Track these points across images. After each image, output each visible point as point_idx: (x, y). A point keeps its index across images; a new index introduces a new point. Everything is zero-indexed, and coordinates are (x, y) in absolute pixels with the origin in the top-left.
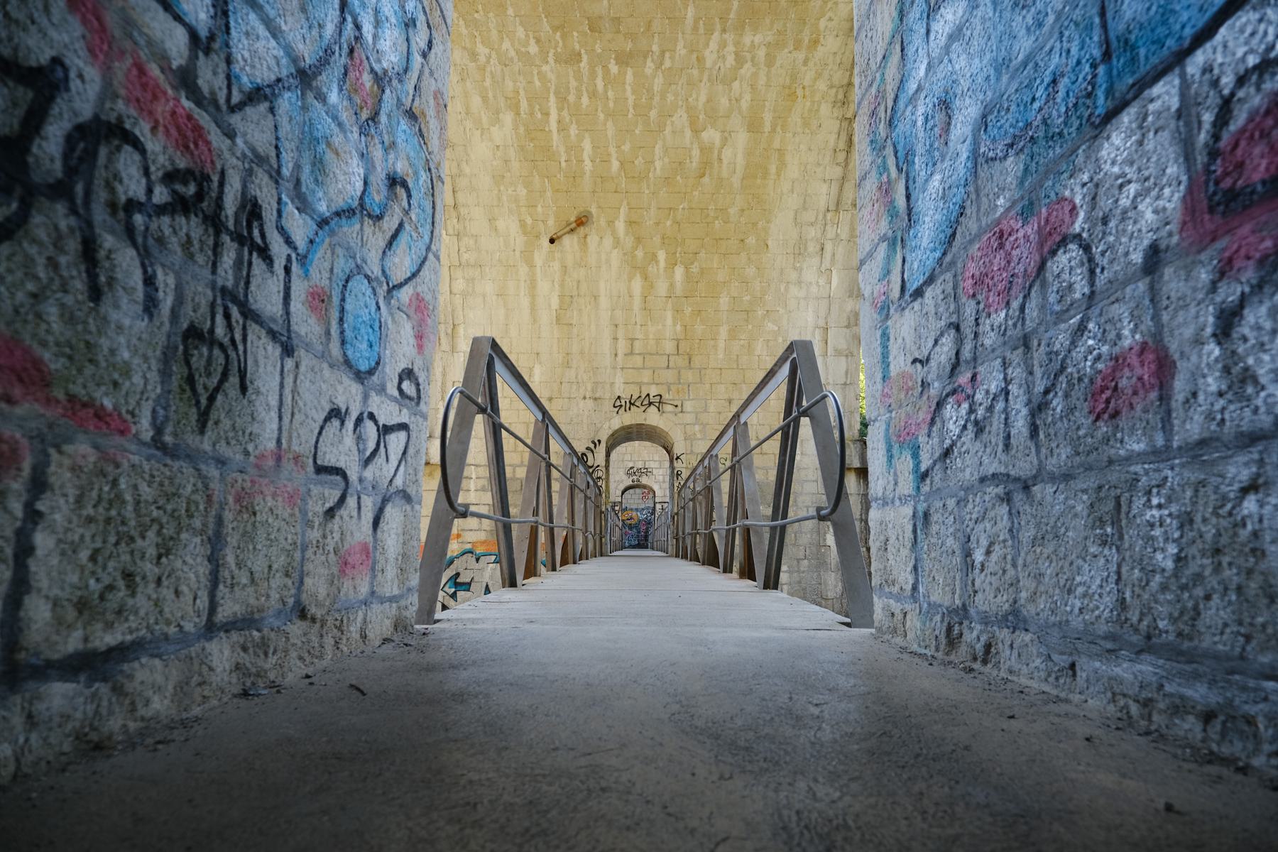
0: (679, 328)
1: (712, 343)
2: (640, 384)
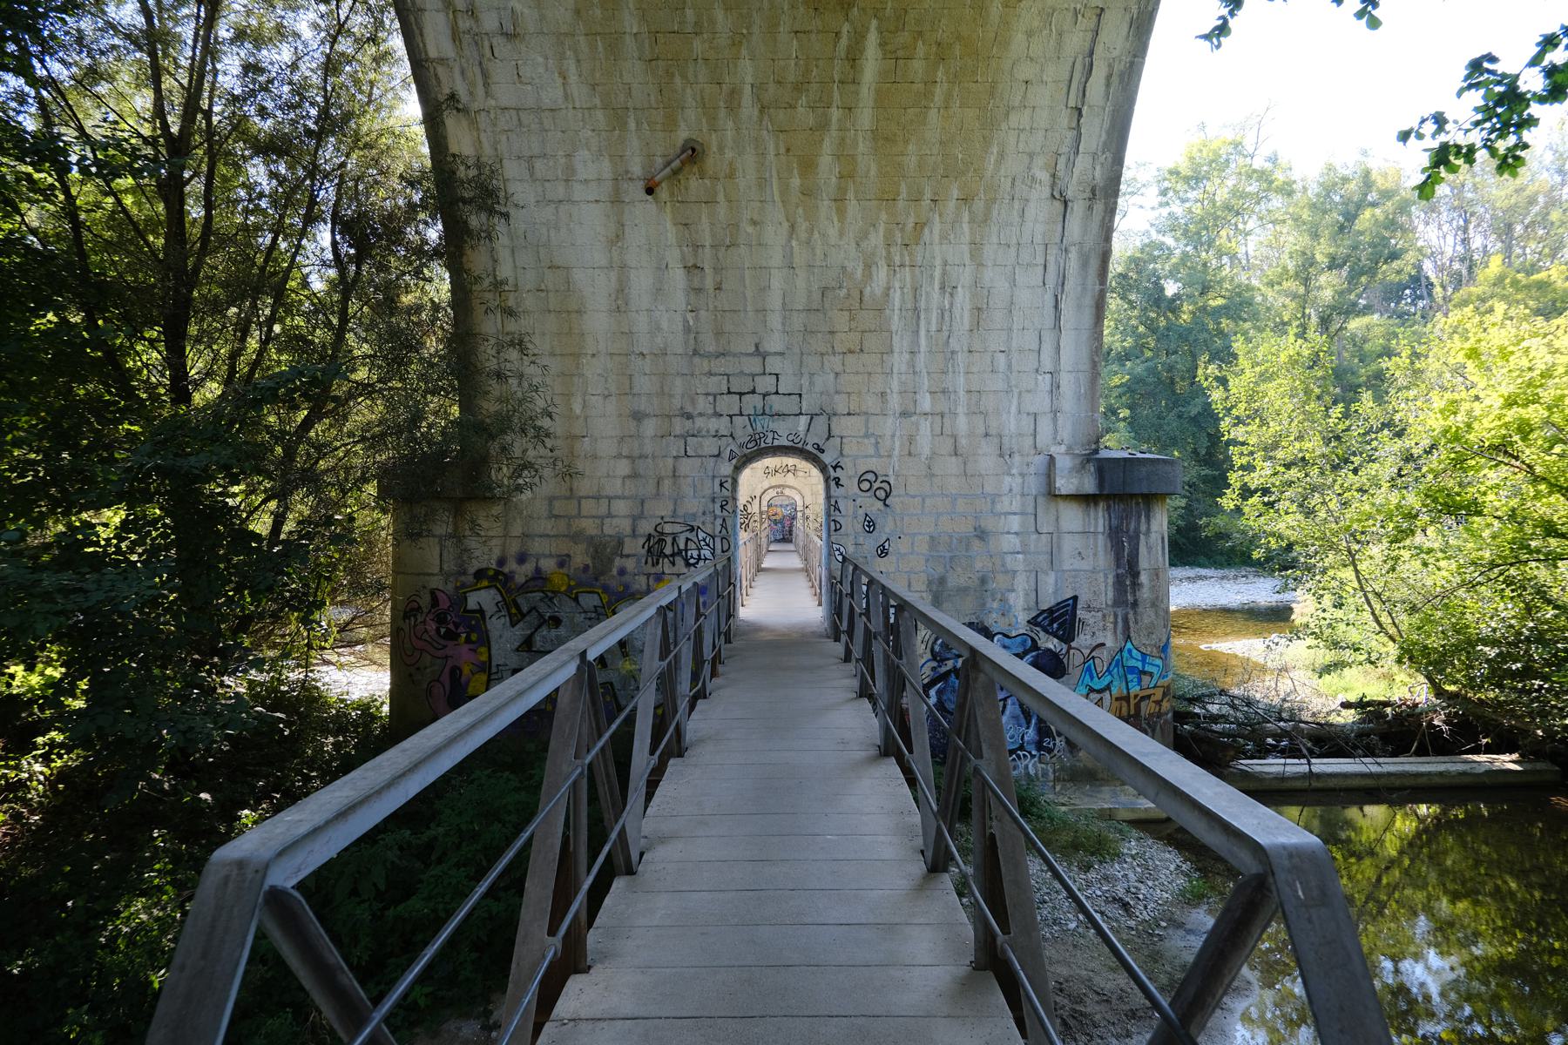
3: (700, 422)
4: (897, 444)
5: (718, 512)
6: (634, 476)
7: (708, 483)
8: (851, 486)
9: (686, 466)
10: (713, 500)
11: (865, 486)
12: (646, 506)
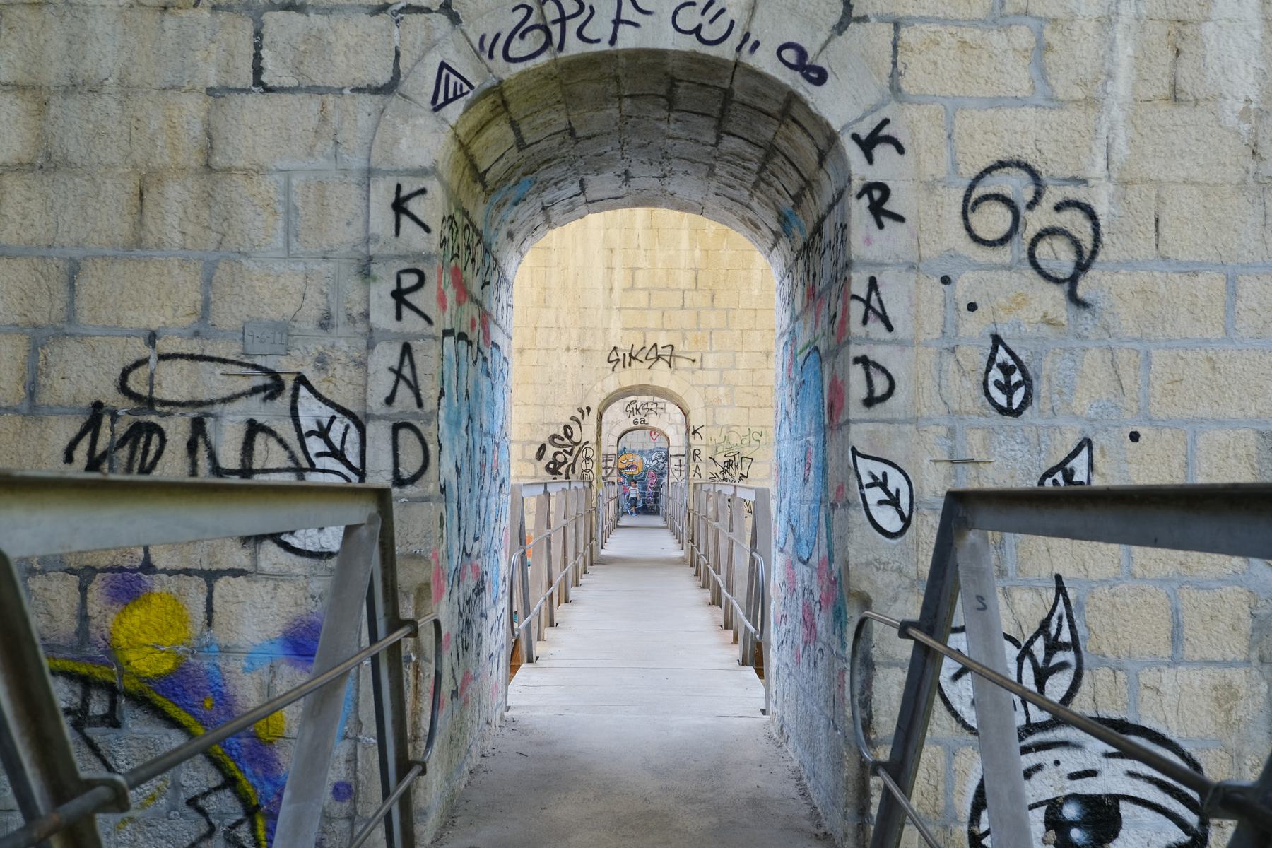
0: (697, 253)
1: (743, 273)
2: (644, 331)
4: (1125, 51)
5: (383, 315)
6: (45, 163)
7: (346, 198)
8: (930, 218)
9: (256, 128)
10: (365, 272)
11: (993, 220)
12: (87, 286)
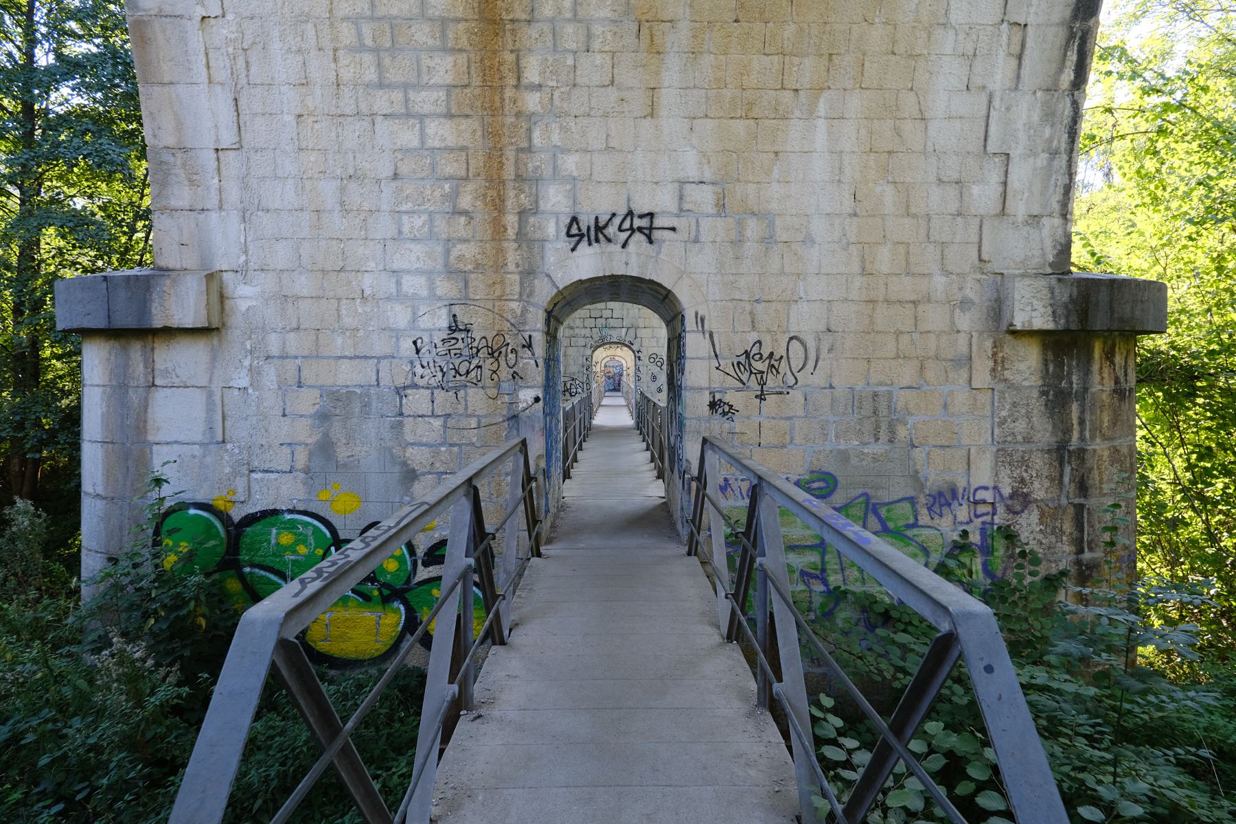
3: (577, 331)
8: (645, 360)
